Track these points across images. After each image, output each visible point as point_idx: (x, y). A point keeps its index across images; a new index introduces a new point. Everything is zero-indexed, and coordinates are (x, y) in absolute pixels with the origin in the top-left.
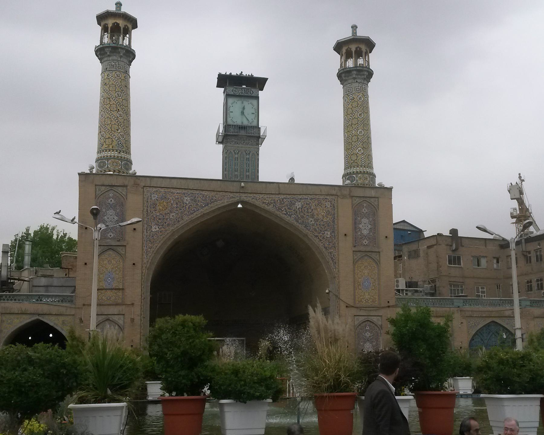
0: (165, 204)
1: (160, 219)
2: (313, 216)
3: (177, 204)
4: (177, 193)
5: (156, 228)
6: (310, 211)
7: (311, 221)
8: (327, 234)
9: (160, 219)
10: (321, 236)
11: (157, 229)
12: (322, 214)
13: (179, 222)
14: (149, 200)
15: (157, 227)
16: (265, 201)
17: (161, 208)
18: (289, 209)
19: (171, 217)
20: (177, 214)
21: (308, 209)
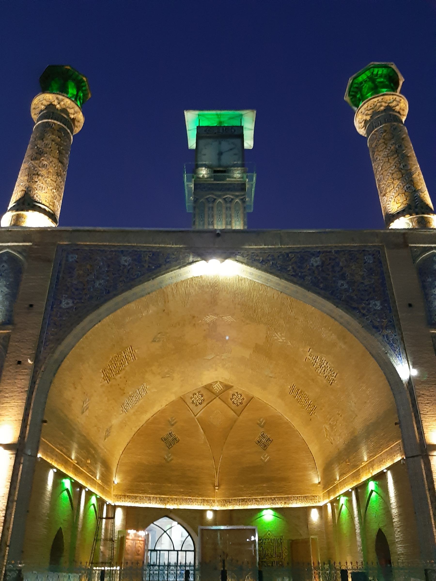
0: (88, 267)
1: (77, 289)
2: (343, 277)
3: (109, 266)
4: (112, 251)
5: (68, 303)
6: (337, 269)
7: (342, 285)
8: (375, 305)
9: (77, 289)
10: (363, 308)
11: (71, 305)
12: (361, 273)
13: (109, 292)
14: (63, 262)
15: (70, 301)
16: (257, 258)
17: (81, 272)
18: (299, 267)
19: (97, 285)
20: (108, 281)
21: (333, 267)
